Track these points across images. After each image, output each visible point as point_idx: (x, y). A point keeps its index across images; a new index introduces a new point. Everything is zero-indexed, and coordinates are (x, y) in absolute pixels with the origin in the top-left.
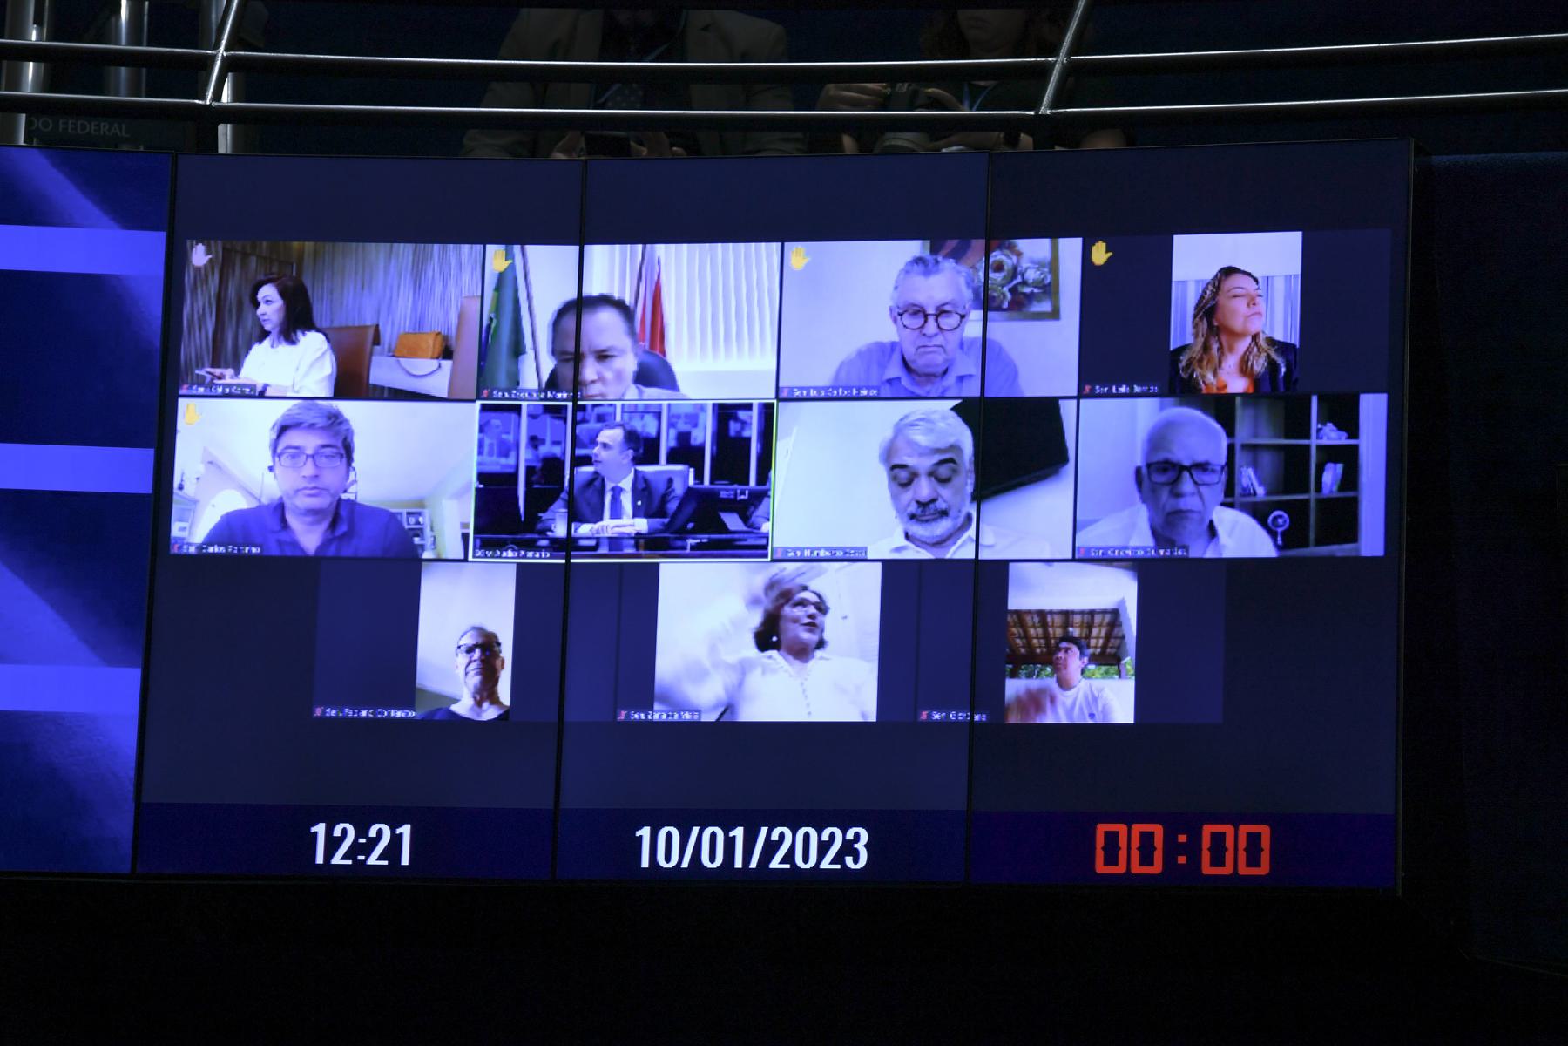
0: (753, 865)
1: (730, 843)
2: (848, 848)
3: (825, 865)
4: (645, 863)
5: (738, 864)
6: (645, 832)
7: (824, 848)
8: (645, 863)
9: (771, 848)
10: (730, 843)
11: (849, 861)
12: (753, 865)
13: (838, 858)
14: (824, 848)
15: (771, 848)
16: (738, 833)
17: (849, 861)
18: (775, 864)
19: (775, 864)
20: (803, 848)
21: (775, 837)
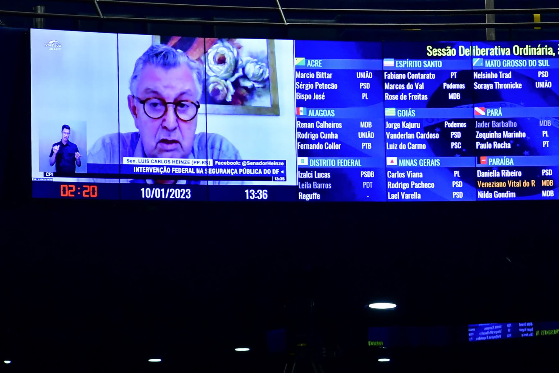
0: (167, 197)
1: (161, 192)
2: (186, 194)
3: (182, 197)
4: (143, 197)
5: (163, 197)
6: (143, 190)
7: (181, 193)
8: (143, 197)
9: (170, 193)
10: (161, 192)
11: (187, 196)
12: (167, 197)
13: (184, 196)
14: (181, 193)
15: (170, 193)
16: (163, 190)
17: (187, 196)
18: (171, 197)
19: (171, 197)
20: (177, 194)
21: (171, 191)
